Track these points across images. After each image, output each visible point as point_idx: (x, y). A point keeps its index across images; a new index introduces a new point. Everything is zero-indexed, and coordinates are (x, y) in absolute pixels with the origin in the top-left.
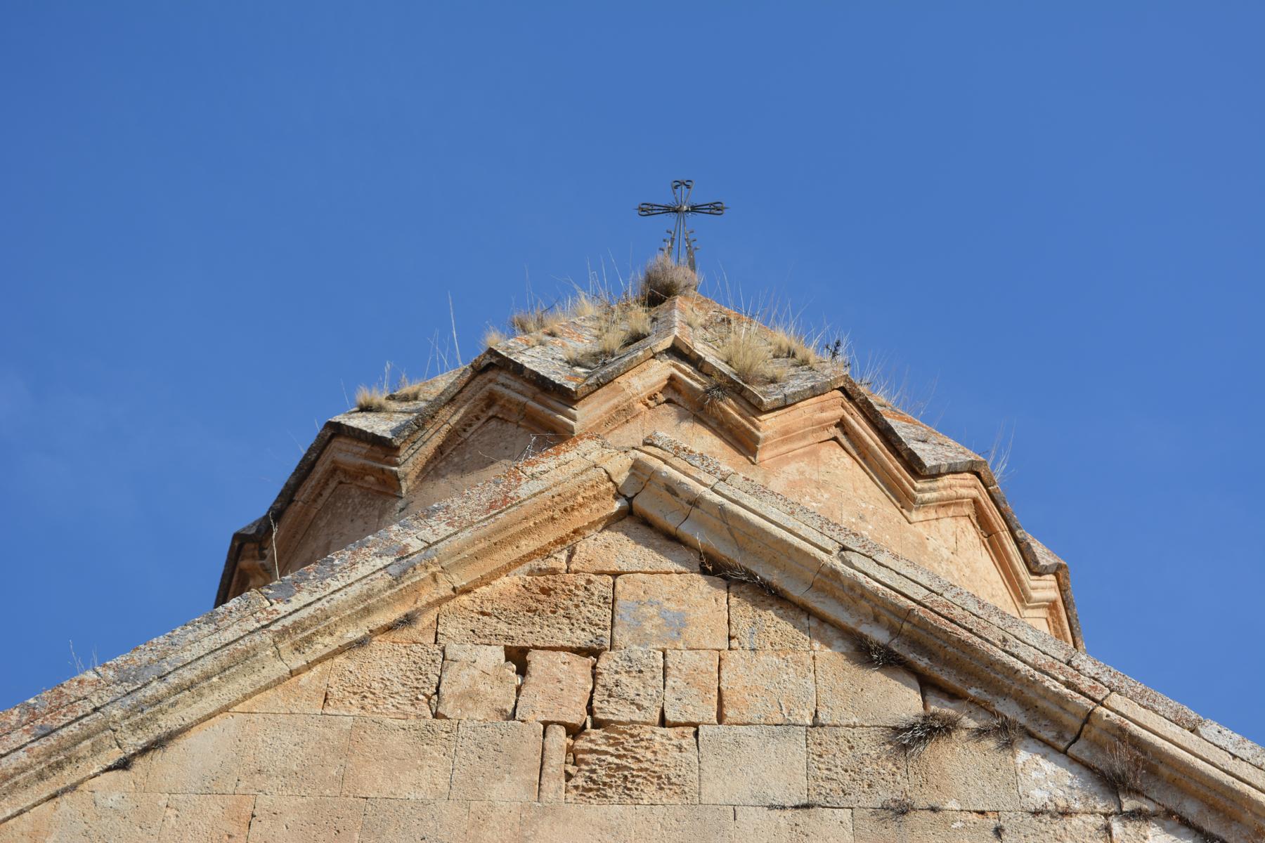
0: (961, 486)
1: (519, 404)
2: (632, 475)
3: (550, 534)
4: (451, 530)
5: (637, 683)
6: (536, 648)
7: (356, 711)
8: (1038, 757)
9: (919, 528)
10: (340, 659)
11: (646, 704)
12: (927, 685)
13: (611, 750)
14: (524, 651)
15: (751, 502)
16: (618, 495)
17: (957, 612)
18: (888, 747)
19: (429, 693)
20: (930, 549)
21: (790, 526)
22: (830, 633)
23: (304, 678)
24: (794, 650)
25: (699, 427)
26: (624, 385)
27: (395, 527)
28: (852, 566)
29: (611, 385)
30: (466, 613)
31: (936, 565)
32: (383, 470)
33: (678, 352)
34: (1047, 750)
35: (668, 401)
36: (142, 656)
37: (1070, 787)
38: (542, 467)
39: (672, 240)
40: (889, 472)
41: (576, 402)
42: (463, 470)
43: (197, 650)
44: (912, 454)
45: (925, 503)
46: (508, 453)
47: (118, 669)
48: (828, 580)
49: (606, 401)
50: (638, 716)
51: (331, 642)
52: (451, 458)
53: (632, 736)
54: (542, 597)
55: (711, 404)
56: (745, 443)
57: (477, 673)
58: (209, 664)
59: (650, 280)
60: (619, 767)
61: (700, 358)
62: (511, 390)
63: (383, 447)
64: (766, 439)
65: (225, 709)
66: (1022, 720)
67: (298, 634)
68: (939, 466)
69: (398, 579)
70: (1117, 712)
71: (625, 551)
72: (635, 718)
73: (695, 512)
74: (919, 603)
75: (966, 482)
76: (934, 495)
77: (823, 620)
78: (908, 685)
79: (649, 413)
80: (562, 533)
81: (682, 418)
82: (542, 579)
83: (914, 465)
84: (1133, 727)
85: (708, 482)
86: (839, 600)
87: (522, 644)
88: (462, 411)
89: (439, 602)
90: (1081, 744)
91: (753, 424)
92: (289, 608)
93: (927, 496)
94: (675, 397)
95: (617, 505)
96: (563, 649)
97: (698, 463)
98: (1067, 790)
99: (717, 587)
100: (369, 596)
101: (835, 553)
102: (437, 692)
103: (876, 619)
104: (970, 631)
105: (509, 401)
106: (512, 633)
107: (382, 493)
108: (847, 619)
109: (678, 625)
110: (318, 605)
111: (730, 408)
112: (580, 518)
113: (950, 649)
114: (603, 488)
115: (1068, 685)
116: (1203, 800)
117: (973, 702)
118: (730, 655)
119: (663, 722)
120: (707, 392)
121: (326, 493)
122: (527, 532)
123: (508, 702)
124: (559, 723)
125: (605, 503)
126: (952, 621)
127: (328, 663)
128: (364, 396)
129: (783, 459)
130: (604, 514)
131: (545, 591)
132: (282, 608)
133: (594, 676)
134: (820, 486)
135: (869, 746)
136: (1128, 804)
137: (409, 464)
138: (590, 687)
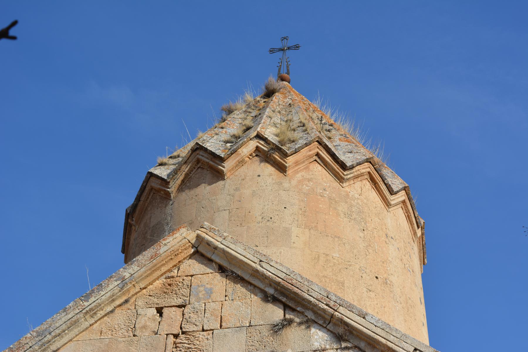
0: (363, 169)
1: (207, 162)
2: (197, 239)
3: (170, 265)
4: (139, 268)
5: (196, 316)
6: (165, 307)
7: (110, 336)
8: (318, 330)
9: (347, 189)
10: (106, 318)
11: (198, 324)
12: (286, 307)
13: (186, 342)
14: (162, 308)
15: (232, 246)
16: (193, 246)
17: (294, 282)
18: (271, 332)
19: (132, 327)
20: (350, 196)
21: (244, 254)
22: (257, 291)
23: (95, 326)
24: (245, 299)
25: (267, 164)
26: (241, 152)
27: (121, 269)
28: (263, 268)
29: (236, 153)
30: (144, 296)
31: (352, 202)
32: (165, 190)
33: (259, 136)
34: (320, 327)
35: (257, 156)
36: (43, 327)
37: (327, 340)
38: (168, 241)
39: (281, 62)
40: (335, 170)
41: (225, 161)
42: (190, 188)
43: (61, 322)
44: (342, 162)
45: (348, 179)
46: (204, 181)
47: (37, 332)
48: (256, 273)
49: (235, 159)
50: (195, 329)
51: (102, 313)
52: (187, 184)
53: (193, 336)
54: (169, 287)
55: (270, 155)
56: (282, 169)
57: (146, 318)
58: (64, 327)
59: (267, 88)
60: (189, 348)
61: (266, 138)
62: (205, 158)
63: (165, 182)
64: (289, 166)
65: (71, 340)
66: (313, 318)
67: (91, 312)
68: (353, 165)
69: (122, 289)
70: (341, 314)
71: (195, 267)
72: (195, 330)
73: (216, 251)
74: (283, 279)
75: (365, 167)
76: (352, 175)
77: (255, 286)
78: (280, 308)
79: (250, 161)
80: (175, 264)
81: (261, 161)
82: (169, 280)
83: (343, 166)
84: (345, 319)
85: (220, 240)
86: (259, 279)
87: (161, 306)
88: (189, 166)
89: (136, 294)
90: (331, 325)
91: (284, 161)
92: (88, 304)
93: (349, 176)
94: (258, 154)
95: (193, 250)
96: (174, 306)
97: (216, 233)
98: (325, 341)
99: (223, 277)
100: (113, 296)
101: (258, 263)
102: (134, 327)
103: (271, 285)
104: (298, 288)
105: (204, 161)
106: (158, 302)
107: (165, 198)
108: (261, 286)
109: (209, 293)
110: (97, 302)
111: (277, 156)
112: (180, 257)
113: (292, 295)
114: (187, 245)
115: (327, 305)
116: (366, 341)
117: (298, 312)
118: (225, 303)
119: (203, 330)
120: (269, 151)
121: (150, 197)
122: (164, 265)
123: (156, 328)
124: (171, 334)
125: (189, 250)
126: (292, 285)
127: (102, 320)
128: (160, 160)
129: (296, 172)
130: (188, 254)
131: (170, 285)
132: (86, 304)
133: (183, 315)
134: (309, 180)
135: (266, 332)
136: (344, 345)
137: (173, 188)
138: (181, 319)
